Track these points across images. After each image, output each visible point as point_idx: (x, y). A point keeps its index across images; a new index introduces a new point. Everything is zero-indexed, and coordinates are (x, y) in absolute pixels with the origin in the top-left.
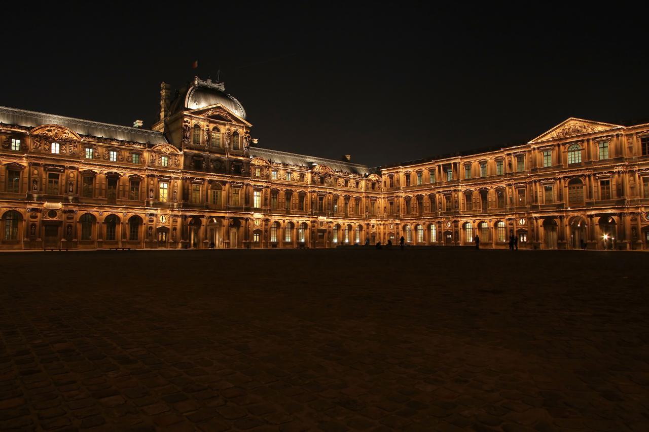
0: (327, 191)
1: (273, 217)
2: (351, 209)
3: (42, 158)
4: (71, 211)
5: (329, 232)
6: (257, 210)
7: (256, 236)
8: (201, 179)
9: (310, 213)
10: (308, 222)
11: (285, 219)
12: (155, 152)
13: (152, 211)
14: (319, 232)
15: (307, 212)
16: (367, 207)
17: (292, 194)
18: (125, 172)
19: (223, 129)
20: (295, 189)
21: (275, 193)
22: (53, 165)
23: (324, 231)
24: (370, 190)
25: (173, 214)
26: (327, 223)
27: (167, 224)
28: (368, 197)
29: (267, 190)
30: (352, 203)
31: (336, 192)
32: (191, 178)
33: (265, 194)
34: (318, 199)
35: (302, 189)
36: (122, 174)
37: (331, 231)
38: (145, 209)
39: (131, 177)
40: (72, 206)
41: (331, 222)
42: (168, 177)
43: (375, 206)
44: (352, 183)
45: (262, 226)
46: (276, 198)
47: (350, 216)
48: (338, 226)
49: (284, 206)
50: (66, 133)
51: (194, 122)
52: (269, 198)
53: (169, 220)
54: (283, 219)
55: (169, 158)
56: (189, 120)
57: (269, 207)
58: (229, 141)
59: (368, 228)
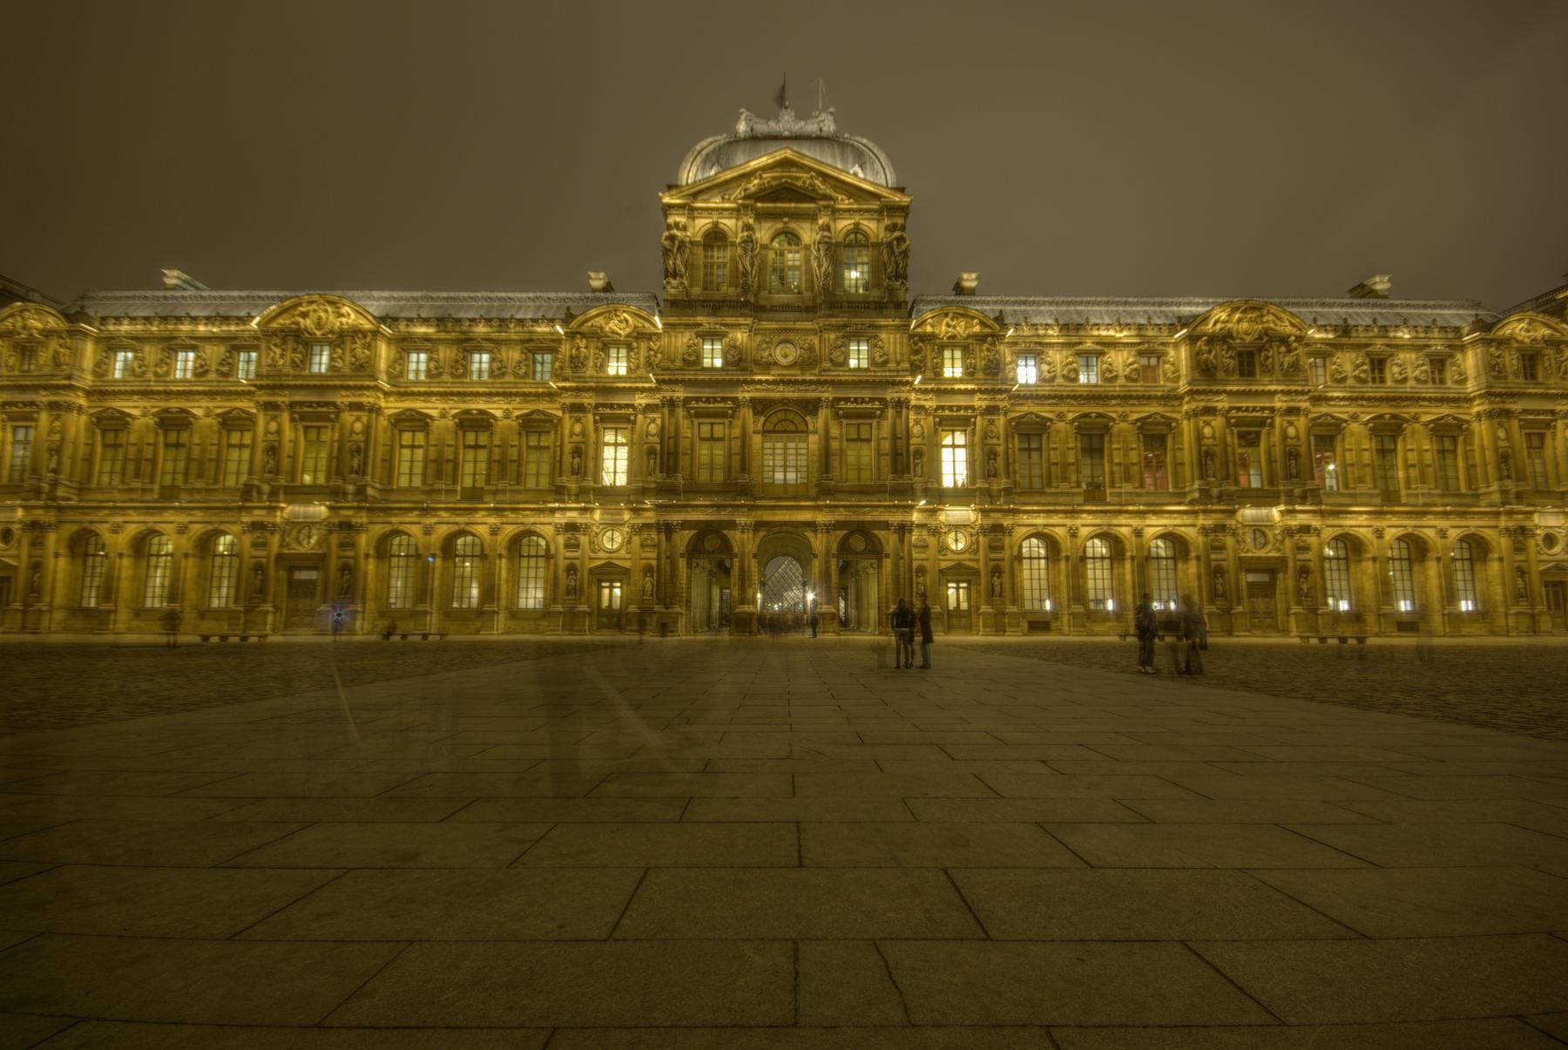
0: (1278, 405)
1: (1025, 519)
2: (1414, 473)
3: (282, 387)
4: (346, 526)
5: (1304, 571)
7: (958, 589)
8: (724, 400)
9: (1196, 495)
10: (1191, 533)
12: (584, 336)
13: (573, 516)
14: (1248, 571)
15: (1184, 494)
16: (1504, 458)
17: (1107, 428)
19: (808, 234)
20: (1120, 409)
21: (1031, 432)
22: (310, 404)
23: (1272, 568)
24: (1515, 382)
25: (640, 521)
26: (1289, 532)
27: (622, 553)
28: (1507, 414)
29: (992, 422)
30: (1417, 446)
31: (1324, 409)
32: (687, 400)
33: (985, 435)
34: (1233, 440)
35: (1154, 408)
37: (1313, 565)
38: (553, 511)
40: (350, 512)
41: (1306, 529)
42: (628, 406)
43: (1548, 452)
44: (1407, 367)
45: (977, 552)
46: (1039, 450)
47: (1412, 500)
48: (1352, 546)
49: (1074, 477)
50: (342, 315)
52: (1001, 449)
53: (629, 542)
54: (1068, 522)
55: (630, 348)
56: (682, 220)
57: (1004, 482)
58: (825, 264)
59: (1520, 549)
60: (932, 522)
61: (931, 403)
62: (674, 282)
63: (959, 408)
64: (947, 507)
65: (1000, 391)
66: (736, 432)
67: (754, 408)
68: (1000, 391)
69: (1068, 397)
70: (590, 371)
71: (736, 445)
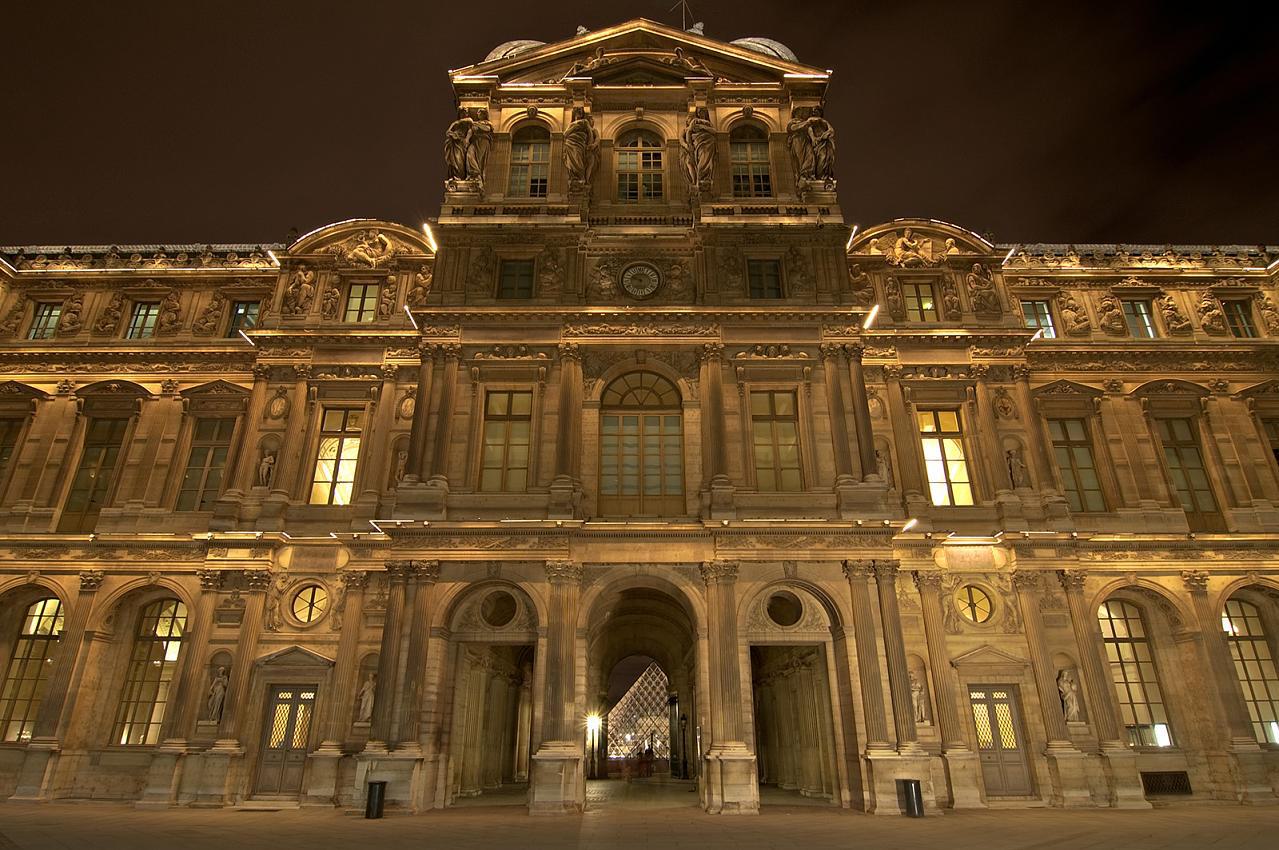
6: (954, 520)
11: (1200, 566)
12: (310, 266)
18: (172, 377)
36: (154, 389)
39: (196, 398)
42: (366, 370)
51: (507, 117)
60: (922, 567)
61: (893, 360)
62: (461, 183)
63: (945, 369)
64: (951, 539)
65: (1012, 341)
66: (553, 403)
67: (585, 364)
68: (1012, 341)
69: (1121, 356)
70: (312, 316)
71: (551, 425)
